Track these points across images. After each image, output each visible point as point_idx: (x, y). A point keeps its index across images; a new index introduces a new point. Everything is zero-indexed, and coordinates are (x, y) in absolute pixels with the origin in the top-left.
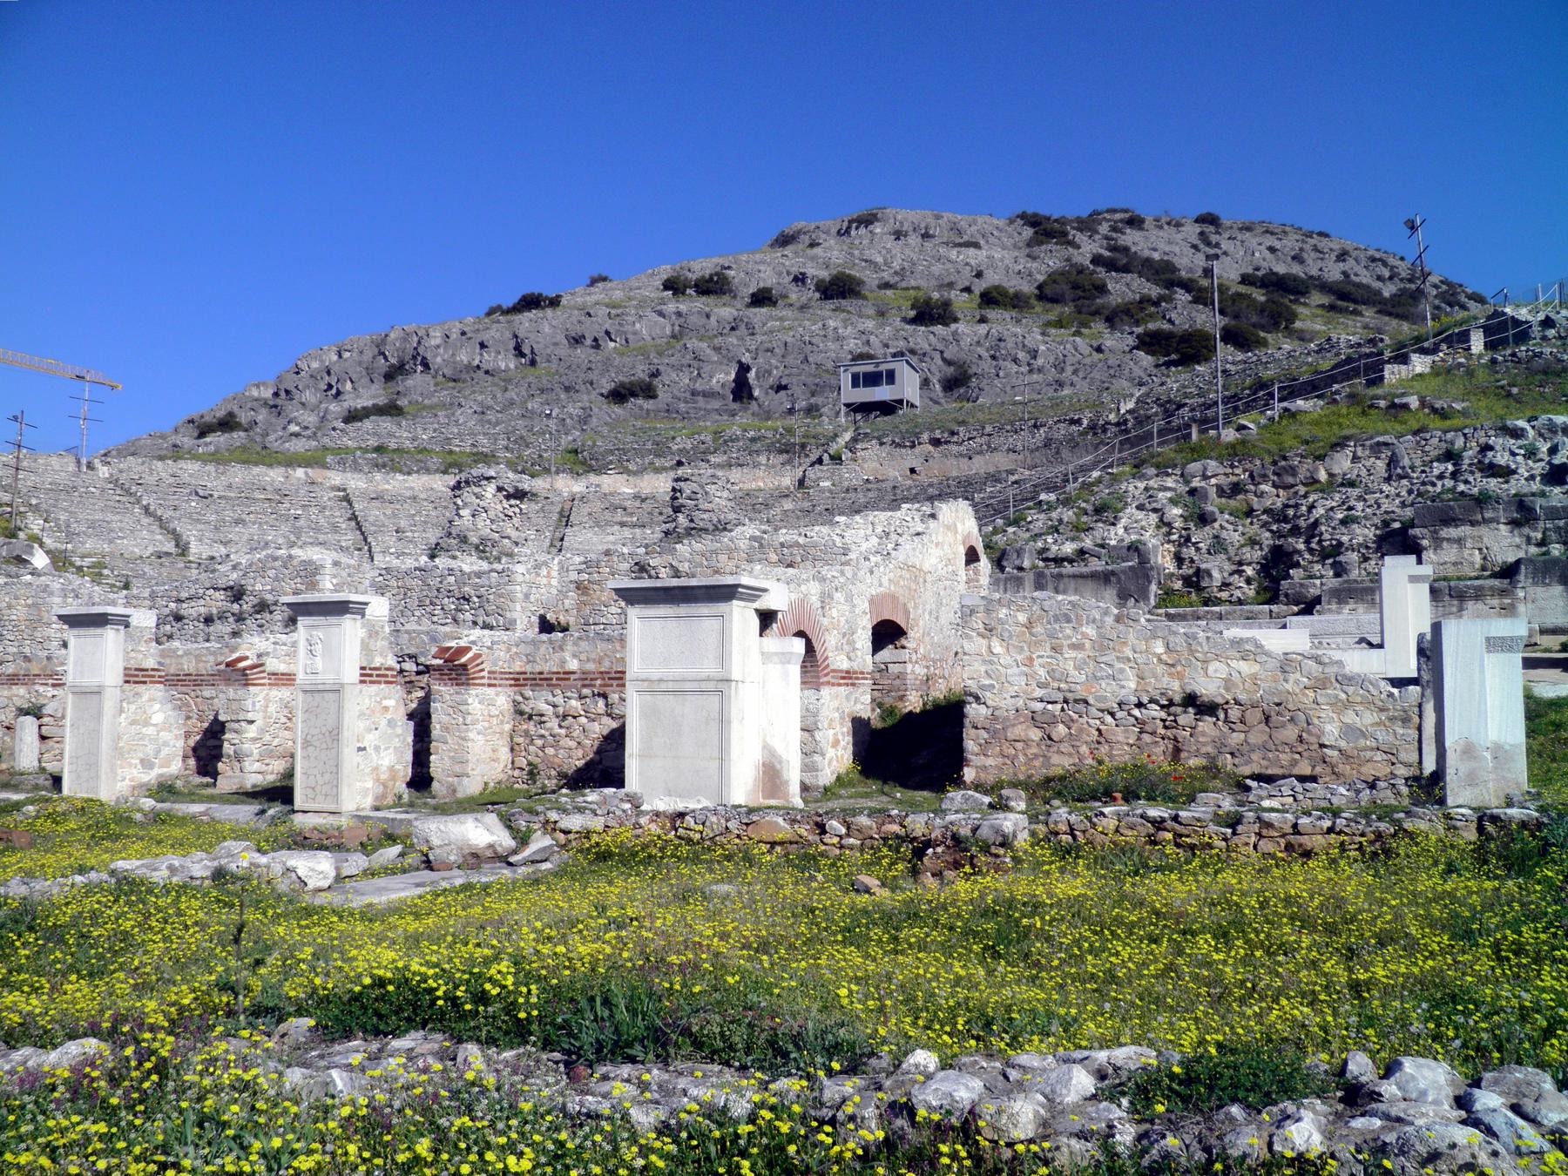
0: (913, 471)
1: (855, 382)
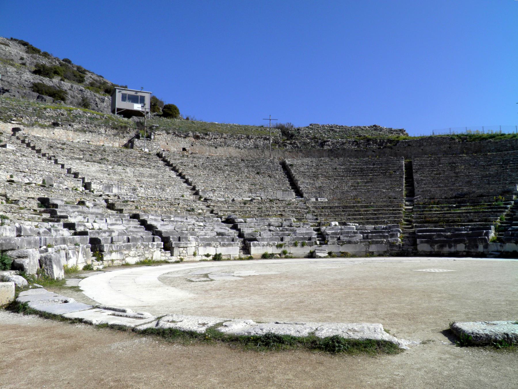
0: (184, 149)
1: (124, 98)
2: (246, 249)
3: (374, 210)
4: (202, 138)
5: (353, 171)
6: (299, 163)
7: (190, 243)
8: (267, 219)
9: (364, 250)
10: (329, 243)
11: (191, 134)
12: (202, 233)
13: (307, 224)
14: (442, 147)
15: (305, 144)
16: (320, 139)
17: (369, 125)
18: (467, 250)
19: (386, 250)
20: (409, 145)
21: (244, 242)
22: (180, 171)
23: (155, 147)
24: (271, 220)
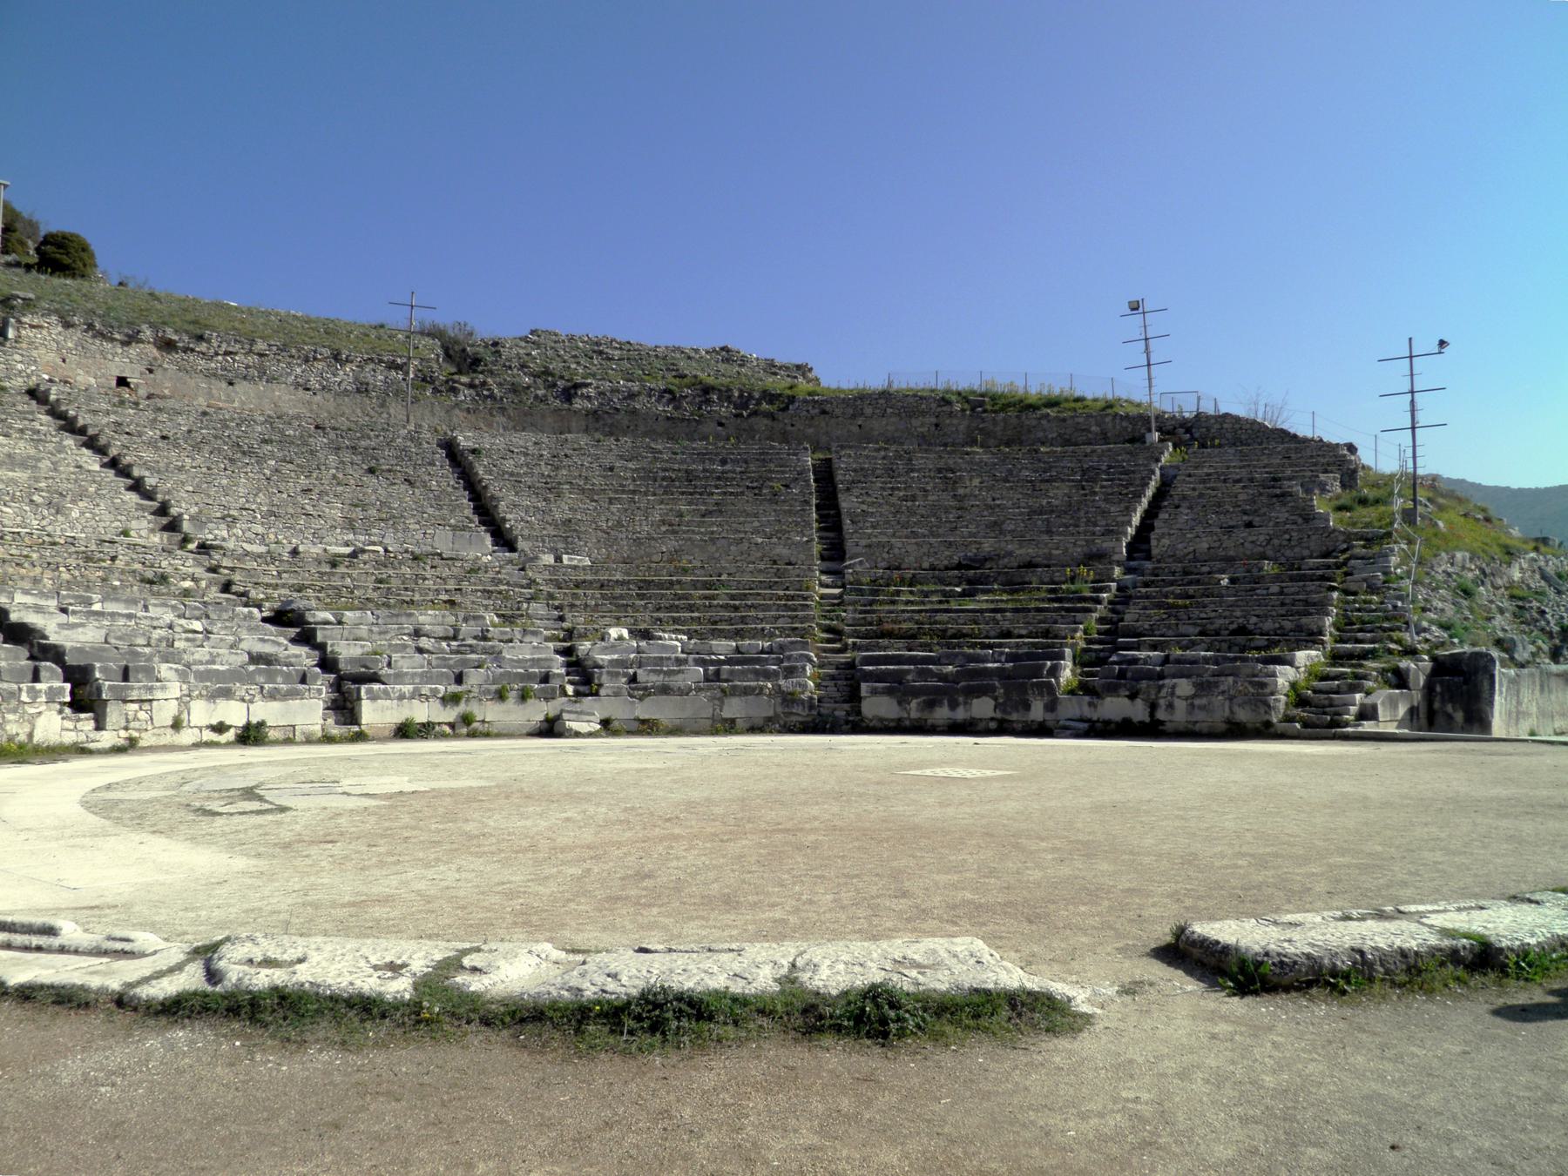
2: (344, 708)
3: (733, 597)
4: (186, 350)
5: (664, 479)
6: (498, 447)
7: (163, 688)
8: (411, 615)
9: (708, 713)
10: (602, 692)
11: (147, 333)
12: (202, 654)
13: (535, 633)
14: (915, 422)
15: (515, 389)
16: (562, 377)
17: (709, 347)
18: (999, 715)
19: (771, 713)
20: (824, 412)
21: (337, 686)
22: (113, 452)
23: (20, 366)
24: (422, 619)
